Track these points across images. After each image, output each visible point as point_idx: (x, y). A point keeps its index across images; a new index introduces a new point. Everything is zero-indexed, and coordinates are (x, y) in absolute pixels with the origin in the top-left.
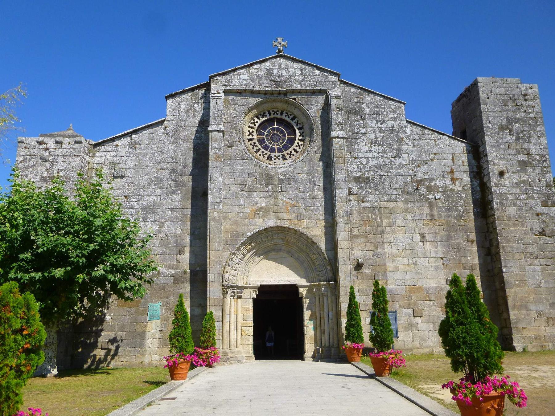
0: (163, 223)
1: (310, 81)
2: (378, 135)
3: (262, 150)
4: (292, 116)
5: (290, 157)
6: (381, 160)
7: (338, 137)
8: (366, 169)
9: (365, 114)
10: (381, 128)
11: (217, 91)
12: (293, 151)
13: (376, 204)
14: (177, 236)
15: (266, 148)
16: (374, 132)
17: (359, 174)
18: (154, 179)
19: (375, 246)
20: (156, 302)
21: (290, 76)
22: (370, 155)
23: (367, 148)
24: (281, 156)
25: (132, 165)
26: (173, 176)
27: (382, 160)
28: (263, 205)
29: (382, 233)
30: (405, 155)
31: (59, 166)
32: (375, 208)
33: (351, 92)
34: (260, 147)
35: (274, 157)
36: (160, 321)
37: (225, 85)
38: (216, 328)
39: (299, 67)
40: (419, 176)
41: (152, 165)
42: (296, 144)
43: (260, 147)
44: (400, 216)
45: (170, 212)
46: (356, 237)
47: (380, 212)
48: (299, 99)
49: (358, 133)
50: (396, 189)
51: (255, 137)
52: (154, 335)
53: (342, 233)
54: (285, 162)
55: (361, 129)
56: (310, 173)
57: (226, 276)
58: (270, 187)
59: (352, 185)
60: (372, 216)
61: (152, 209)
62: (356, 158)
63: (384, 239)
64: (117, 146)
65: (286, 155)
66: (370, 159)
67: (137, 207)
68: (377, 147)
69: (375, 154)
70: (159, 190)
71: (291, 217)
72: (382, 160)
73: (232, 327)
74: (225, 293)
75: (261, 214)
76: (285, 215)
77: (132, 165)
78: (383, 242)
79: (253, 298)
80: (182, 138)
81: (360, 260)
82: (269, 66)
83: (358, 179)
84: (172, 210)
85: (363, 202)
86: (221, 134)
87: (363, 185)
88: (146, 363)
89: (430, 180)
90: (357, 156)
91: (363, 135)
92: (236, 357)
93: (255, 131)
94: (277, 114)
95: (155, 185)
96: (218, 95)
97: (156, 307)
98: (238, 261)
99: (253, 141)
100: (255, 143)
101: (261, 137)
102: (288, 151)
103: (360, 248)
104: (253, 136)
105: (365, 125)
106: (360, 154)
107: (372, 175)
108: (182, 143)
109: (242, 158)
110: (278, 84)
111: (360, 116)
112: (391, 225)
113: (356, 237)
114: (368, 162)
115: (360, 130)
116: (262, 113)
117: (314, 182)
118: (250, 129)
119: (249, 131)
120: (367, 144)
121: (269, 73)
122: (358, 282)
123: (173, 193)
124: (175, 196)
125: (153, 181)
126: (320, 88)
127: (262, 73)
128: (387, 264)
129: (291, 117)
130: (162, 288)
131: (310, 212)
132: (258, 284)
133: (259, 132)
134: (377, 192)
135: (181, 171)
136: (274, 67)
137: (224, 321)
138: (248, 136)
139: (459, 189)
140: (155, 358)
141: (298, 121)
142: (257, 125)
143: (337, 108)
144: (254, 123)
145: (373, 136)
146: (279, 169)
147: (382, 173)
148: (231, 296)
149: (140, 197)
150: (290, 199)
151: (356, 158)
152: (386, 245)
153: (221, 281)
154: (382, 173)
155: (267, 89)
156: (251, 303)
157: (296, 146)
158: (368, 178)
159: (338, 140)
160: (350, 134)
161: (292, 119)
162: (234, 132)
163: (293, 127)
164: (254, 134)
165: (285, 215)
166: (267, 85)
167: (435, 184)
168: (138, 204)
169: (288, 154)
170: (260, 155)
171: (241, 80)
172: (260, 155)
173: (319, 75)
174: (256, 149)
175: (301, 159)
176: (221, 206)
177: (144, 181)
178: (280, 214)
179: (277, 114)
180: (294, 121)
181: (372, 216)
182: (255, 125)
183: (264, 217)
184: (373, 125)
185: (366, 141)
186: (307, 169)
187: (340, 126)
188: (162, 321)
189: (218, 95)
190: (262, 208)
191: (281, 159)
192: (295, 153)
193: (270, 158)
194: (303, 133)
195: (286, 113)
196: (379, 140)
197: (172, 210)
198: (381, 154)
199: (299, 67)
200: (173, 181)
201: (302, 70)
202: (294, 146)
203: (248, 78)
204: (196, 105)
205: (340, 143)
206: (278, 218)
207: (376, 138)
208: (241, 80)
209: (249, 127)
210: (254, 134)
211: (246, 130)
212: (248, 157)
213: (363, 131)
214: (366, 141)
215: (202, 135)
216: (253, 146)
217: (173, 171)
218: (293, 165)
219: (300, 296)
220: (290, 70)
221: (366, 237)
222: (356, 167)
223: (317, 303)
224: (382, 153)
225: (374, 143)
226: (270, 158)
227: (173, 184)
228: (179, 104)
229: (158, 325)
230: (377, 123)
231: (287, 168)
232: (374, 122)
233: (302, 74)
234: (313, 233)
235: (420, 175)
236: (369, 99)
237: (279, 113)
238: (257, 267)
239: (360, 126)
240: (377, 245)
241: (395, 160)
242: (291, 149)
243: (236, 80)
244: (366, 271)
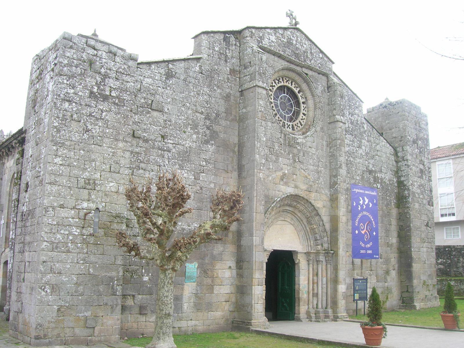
7: (341, 122)
10: (351, 119)
18: (190, 122)
20: (191, 262)
25: (169, 100)
31: (111, 83)
36: (195, 284)
45: (204, 163)
52: (190, 298)
53: (342, 209)
67: (174, 150)
77: (169, 100)
108: (215, 88)
110: (297, 56)
123: (207, 142)
124: (209, 146)
125: (189, 124)
136: (293, 38)
142: (275, 88)
149: (177, 139)
150: (304, 170)
168: (174, 147)
182: (273, 89)
188: (197, 283)
227: (208, 132)
229: (194, 288)
237: (290, 82)
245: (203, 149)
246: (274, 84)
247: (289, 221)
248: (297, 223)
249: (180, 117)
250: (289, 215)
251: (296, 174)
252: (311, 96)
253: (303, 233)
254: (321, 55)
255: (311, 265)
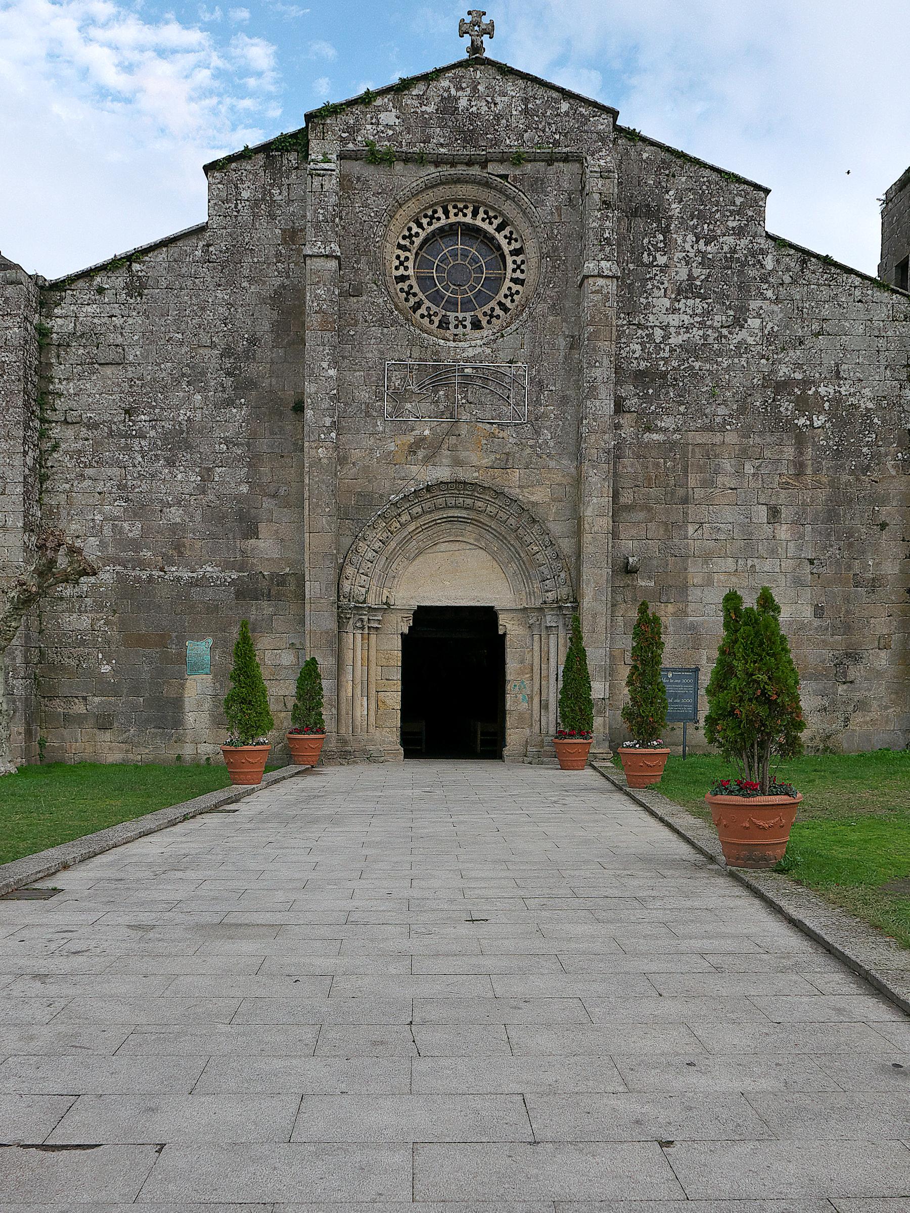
0: (209, 470)
1: (544, 131)
2: (696, 272)
3: (427, 303)
4: (500, 220)
5: (489, 322)
6: (697, 334)
8: (662, 355)
9: (671, 217)
10: (704, 254)
11: (325, 155)
12: (497, 308)
13: (677, 436)
14: (239, 499)
15: (436, 298)
16: (687, 264)
17: (643, 365)
19: (666, 530)
21: (498, 117)
22: (674, 320)
23: (667, 303)
24: (469, 319)
25: (136, 337)
26: (228, 363)
27: (701, 333)
28: (427, 432)
29: (685, 501)
30: (754, 323)
32: (673, 444)
33: (642, 160)
34: (423, 298)
35: (453, 323)
37: (342, 140)
38: (323, 693)
39: (521, 94)
40: (781, 374)
41: (180, 336)
42: (504, 290)
43: (421, 295)
44: (728, 465)
46: (628, 508)
47: (684, 456)
48: (515, 177)
49: (651, 265)
50: (725, 402)
51: (411, 272)
54: (477, 334)
55: (658, 255)
56: (534, 360)
57: (346, 586)
58: (441, 393)
59: (627, 390)
60: (665, 463)
61: (185, 439)
62: (639, 326)
63: (687, 513)
64: (101, 291)
65: (481, 316)
66: (672, 330)
67: (152, 433)
68: (690, 302)
69: (686, 318)
70: (198, 397)
71: (486, 462)
72: (701, 333)
73: (358, 691)
74: (341, 621)
75: (421, 454)
76: (474, 457)
77: (136, 337)
78: (686, 522)
79: (402, 634)
80: (246, 272)
81: (631, 560)
82: (448, 90)
83: (640, 377)
84: (227, 441)
85: (648, 429)
86: (334, 264)
87: (651, 391)
88: (188, 758)
89: (806, 383)
90: (643, 322)
91: (661, 271)
92: (365, 751)
93: (412, 258)
94: (465, 215)
95: (189, 383)
96: (326, 166)
97: (200, 649)
98: (370, 554)
99: (408, 283)
100: (411, 287)
101: (425, 272)
102: (486, 308)
103: (633, 532)
104: (406, 268)
105: (667, 247)
106: (651, 318)
107: (674, 369)
108: (245, 284)
109: (381, 323)
111: (660, 222)
112: (705, 484)
113: (628, 508)
114: (666, 337)
115: (655, 259)
116: (430, 213)
117: (540, 382)
118: (400, 252)
119: (398, 257)
120: (669, 292)
121: (448, 106)
122: (623, 606)
123: (229, 403)
124: (235, 411)
125: (183, 375)
126: (565, 150)
127: (430, 109)
128: (690, 570)
129: (496, 222)
130: (213, 609)
131: (529, 450)
132: (414, 604)
133: (421, 263)
134: (682, 409)
135: (246, 351)
136: (460, 93)
137: (343, 679)
138: (397, 268)
139: (870, 405)
140: (206, 749)
141: (511, 233)
142: (417, 241)
143: (604, 202)
144: (411, 236)
145: (683, 274)
146: (464, 350)
147: (697, 365)
148: (355, 627)
149: (157, 411)
151: (639, 326)
152: (691, 529)
153: (334, 598)
154: (697, 365)
155: (442, 150)
156: (398, 643)
157: (506, 296)
158: (664, 375)
159: (601, 282)
160: (631, 266)
161: (499, 229)
162: (364, 259)
163: (499, 248)
164: (410, 264)
165: (474, 457)
166: (442, 140)
167: (816, 392)
168: (154, 427)
169: (485, 314)
170: (422, 316)
171: (381, 128)
172: (422, 316)
173: (567, 114)
174: (412, 301)
175: (513, 327)
176: (333, 435)
177: (164, 374)
178: (463, 455)
179: (465, 215)
180: (503, 233)
181: (665, 463)
182: (412, 243)
183: (427, 460)
184: (688, 247)
185: (666, 285)
186: (526, 351)
187: (607, 249)
188: (215, 676)
189: (326, 166)
190: (423, 439)
191: (469, 326)
192: (501, 313)
193: (444, 324)
194: (523, 262)
195: (486, 212)
196: (699, 283)
197: (227, 441)
198: (697, 319)
199: (521, 94)
200: (228, 374)
201: (525, 101)
202: (500, 297)
203: (397, 121)
204: (276, 191)
205: (605, 291)
206: (457, 463)
207: (691, 277)
208: (381, 128)
209: (400, 246)
210: (410, 264)
211: (391, 254)
212: (395, 322)
213: (662, 260)
214: (666, 285)
215: (292, 266)
216: (408, 293)
217: (227, 352)
218: (495, 341)
219: (501, 632)
220: (498, 99)
221: (649, 510)
222: (638, 347)
223: (536, 647)
224: (702, 315)
225: (686, 290)
226: (444, 324)
227: (228, 382)
228: (237, 187)
230: (697, 242)
231: (479, 350)
232: (691, 238)
233: (526, 111)
234: (533, 499)
235: (783, 371)
236: (684, 179)
237: (469, 212)
238: (411, 569)
239: (657, 249)
240: (672, 527)
241: (730, 333)
242: (493, 304)
243: (369, 127)
244: (643, 584)
245: (218, 419)
246: (415, 229)
247: (472, 541)
248: (495, 546)
249: (163, 366)
250: (469, 528)
251: (457, 433)
252: (530, 230)
253: (513, 567)
254: (565, 106)
255: (536, 638)
